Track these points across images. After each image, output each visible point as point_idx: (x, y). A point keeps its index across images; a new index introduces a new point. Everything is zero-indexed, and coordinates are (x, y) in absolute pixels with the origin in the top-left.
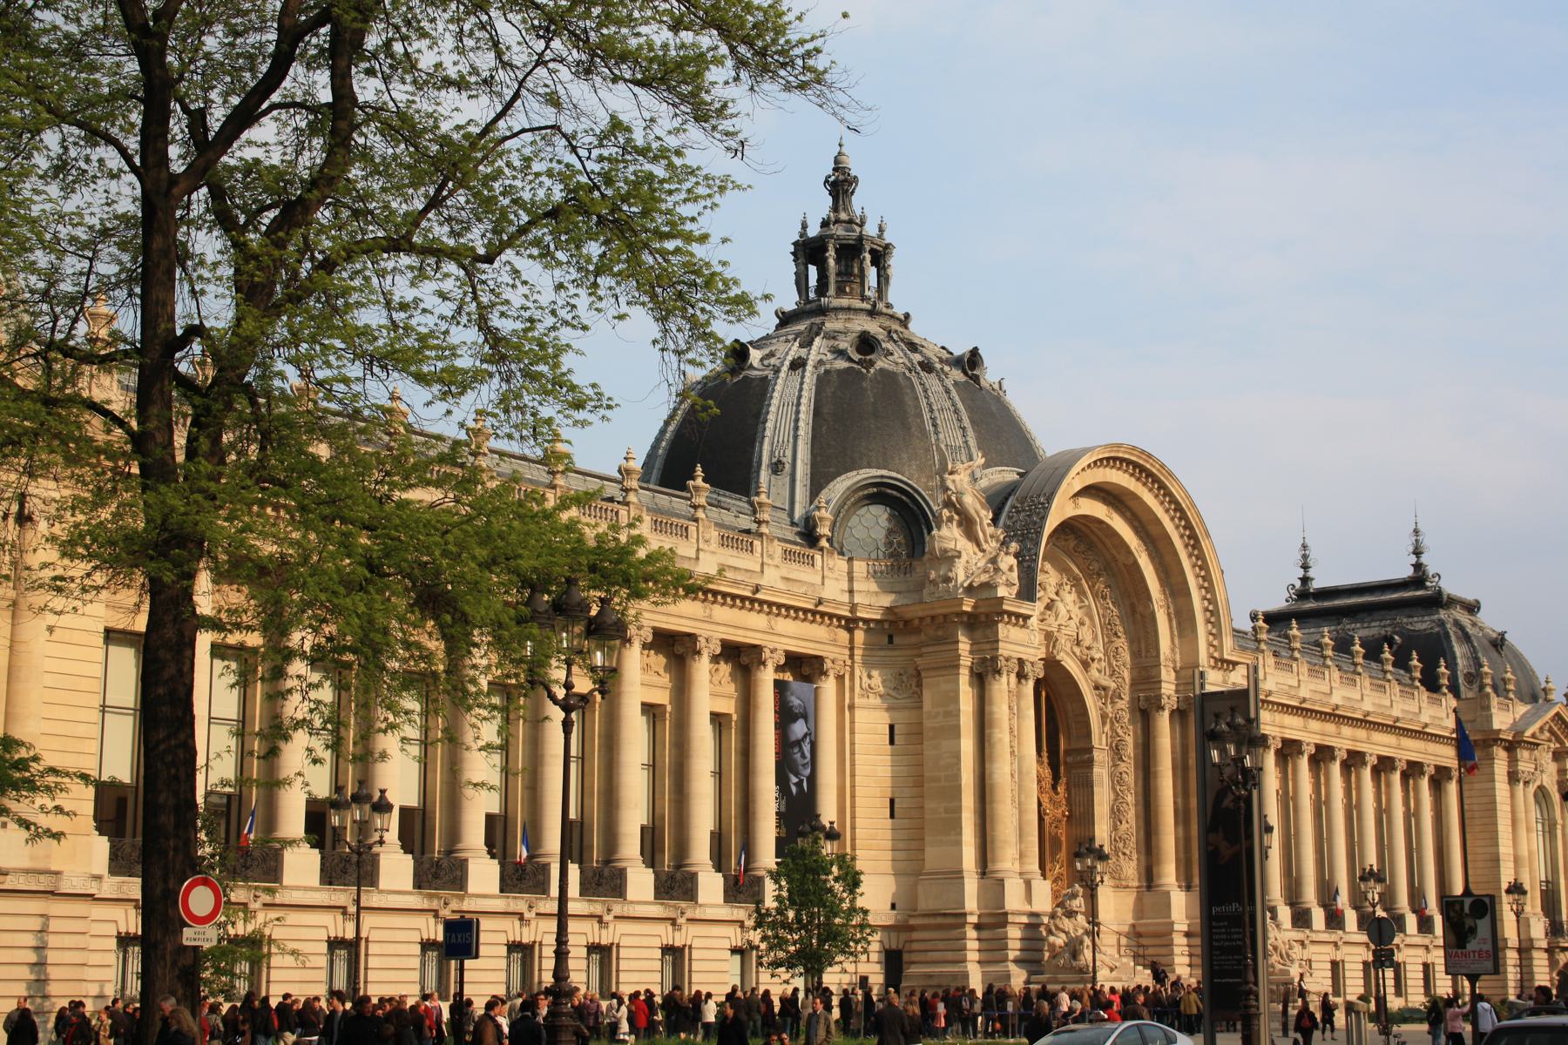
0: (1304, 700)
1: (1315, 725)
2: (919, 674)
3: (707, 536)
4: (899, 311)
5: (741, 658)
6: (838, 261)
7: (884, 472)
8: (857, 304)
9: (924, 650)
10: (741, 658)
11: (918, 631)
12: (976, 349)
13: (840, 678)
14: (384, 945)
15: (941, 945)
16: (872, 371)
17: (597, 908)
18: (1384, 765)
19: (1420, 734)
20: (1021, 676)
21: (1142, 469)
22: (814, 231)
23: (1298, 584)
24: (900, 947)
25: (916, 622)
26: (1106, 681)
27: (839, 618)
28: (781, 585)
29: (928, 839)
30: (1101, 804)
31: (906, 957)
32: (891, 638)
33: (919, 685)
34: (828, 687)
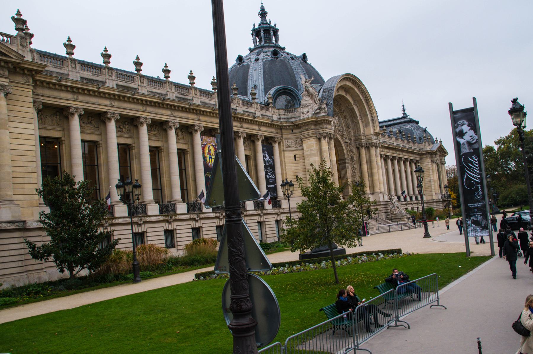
2: (301, 140)
4: (282, 46)
5: (251, 139)
8: (271, 45)
9: (302, 133)
10: (251, 139)
11: (300, 128)
12: (305, 53)
13: (279, 143)
14: (152, 233)
16: (278, 60)
18: (406, 160)
19: (412, 153)
22: (257, 27)
25: (300, 125)
26: (347, 141)
27: (278, 126)
30: (349, 173)
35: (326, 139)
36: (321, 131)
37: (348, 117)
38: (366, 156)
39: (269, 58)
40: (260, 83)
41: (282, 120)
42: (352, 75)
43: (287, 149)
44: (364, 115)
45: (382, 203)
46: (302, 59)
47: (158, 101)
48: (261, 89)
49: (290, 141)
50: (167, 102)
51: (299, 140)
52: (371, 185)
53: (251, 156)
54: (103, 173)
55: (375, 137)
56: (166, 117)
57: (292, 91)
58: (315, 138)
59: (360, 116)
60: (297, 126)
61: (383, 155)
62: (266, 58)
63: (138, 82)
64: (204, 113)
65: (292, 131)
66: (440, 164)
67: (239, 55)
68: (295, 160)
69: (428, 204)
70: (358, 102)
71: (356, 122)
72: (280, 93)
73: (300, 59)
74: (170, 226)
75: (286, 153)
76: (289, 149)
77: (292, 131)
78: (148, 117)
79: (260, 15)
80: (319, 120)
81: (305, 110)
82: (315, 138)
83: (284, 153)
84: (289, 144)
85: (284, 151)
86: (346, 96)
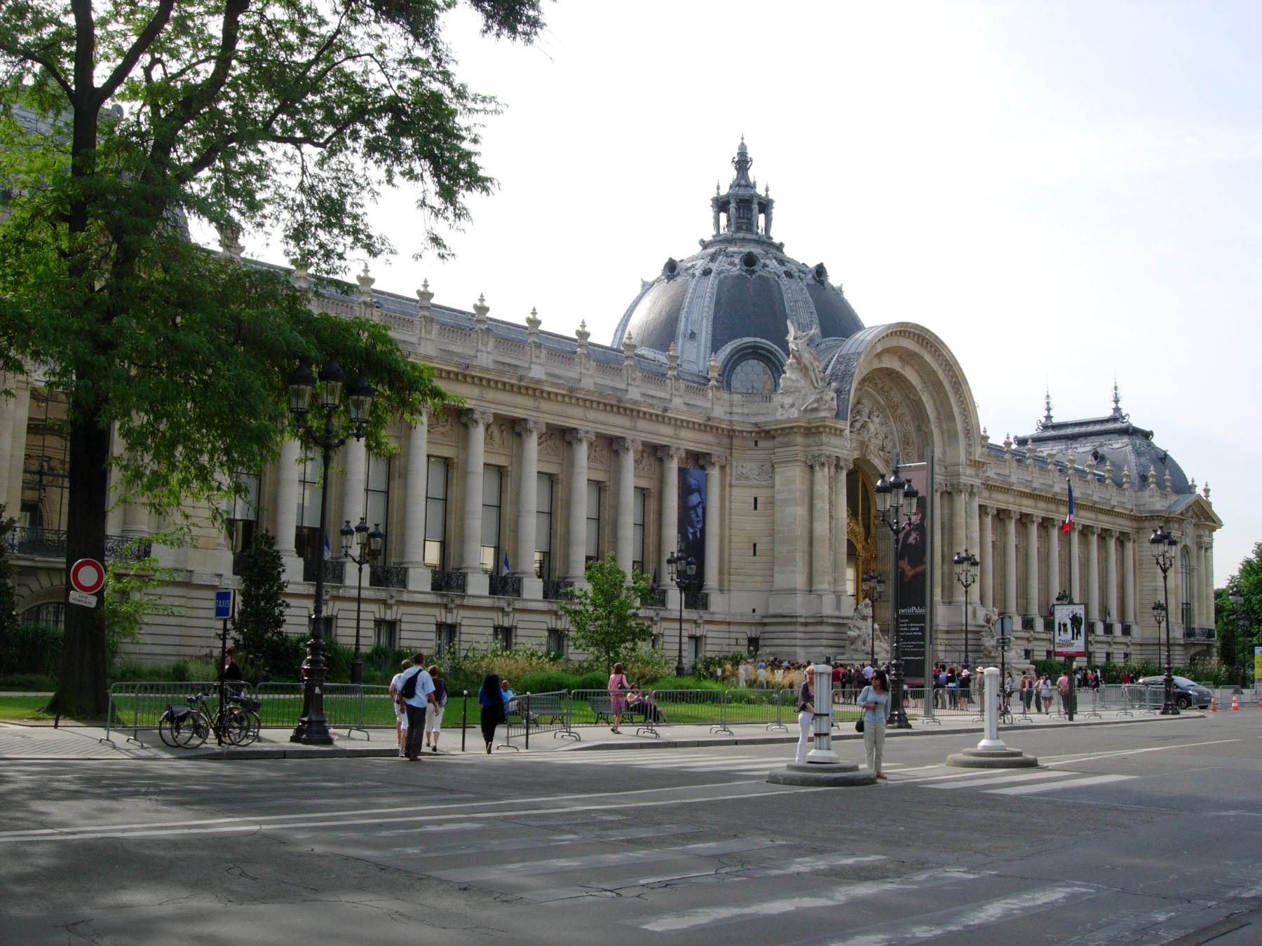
0: (1035, 489)
1: (1042, 505)
2: (773, 466)
3: (634, 376)
4: (776, 240)
6: (738, 209)
7: (758, 339)
8: (749, 236)
10: (657, 453)
13: (723, 468)
15: (782, 635)
17: (554, 607)
19: (1109, 512)
20: (838, 467)
22: (724, 191)
23: (1043, 420)
24: (335, 614)
27: (723, 429)
28: (683, 408)
29: (776, 569)
31: (761, 642)
32: (756, 442)
33: (773, 472)
34: (714, 474)
35: (826, 469)
36: (815, 450)
37: (908, 418)
38: (942, 514)
39: (735, 271)
40: (704, 329)
41: (735, 418)
42: (916, 326)
46: (813, 277)
47: (455, 370)
48: (703, 342)
49: (749, 465)
50: (473, 373)
51: (768, 464)
52: (946, 583)
54: (333, 499)
55: (969, 471)
57: (772, 353)
58: (803, 464)
59: (938, 417)
60: (765, 434)
62: (728, 271)
63: (421, 330)
64: (550, 396)
66: (1193, 548)
67: (670, 259)
68: (756, 508)
69: (1144, 648)
70: (936, 387)
71: (925, 433)
72: (746, 354)
73: (810, 276)
74: (449, 615)
75: (735, 491)
79: (737, 163)
81: (788, 400)
83: (731, 491)
85: (731, 486)
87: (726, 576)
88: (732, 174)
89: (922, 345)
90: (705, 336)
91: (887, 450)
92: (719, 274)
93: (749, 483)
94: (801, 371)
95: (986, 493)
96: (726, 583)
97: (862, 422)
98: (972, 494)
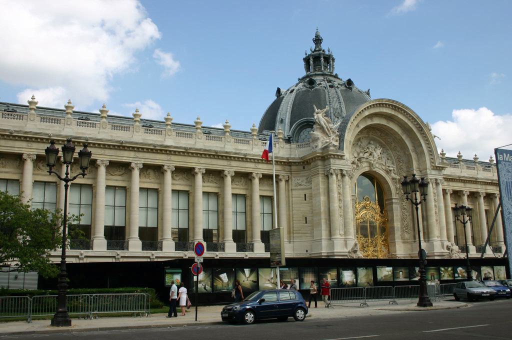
13: (287, 181)
16: (313, 90)
21: (396, 107)
27: (284, 162)
37: (398, 149)
39: (304, 89)
43: (296, 188)
44: (417, 145)
45: (436, 254)
49: (302, 179)
52: (426, 231)
53: (248, 195)
55: (434, 172)
56: (128, 159)
61: (482, 193)
65: (304, 168)
68: (305, 200)
71: (408, 155)
75: (294, 192)
76: (299, 187)
77: (304, 168)
78: (105, 159)
80: (324, 154)
82: (323, 175)
83: (292, 193)
84: (299, 182)
86: (388, 125)
87: (292, 235)
88: (313, 46)
89: (395, 110)
90: (287, 121)
91: (387, 165)
92: (297, 91)
93: (302, 187)
94: (321, 129)
95: (446, 183)
96: (292, 238)
97: (369, 153)
98: (437, 184)
